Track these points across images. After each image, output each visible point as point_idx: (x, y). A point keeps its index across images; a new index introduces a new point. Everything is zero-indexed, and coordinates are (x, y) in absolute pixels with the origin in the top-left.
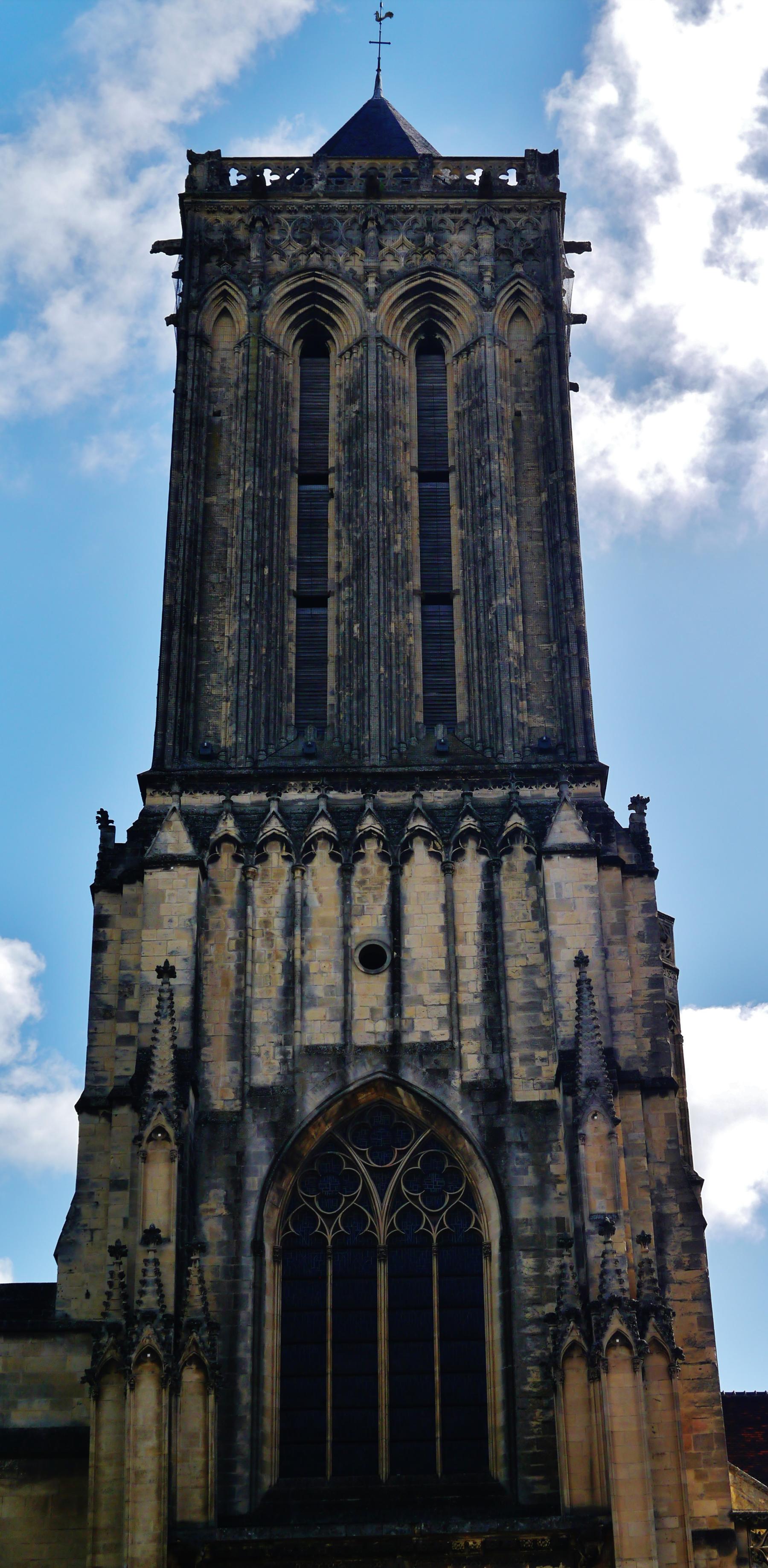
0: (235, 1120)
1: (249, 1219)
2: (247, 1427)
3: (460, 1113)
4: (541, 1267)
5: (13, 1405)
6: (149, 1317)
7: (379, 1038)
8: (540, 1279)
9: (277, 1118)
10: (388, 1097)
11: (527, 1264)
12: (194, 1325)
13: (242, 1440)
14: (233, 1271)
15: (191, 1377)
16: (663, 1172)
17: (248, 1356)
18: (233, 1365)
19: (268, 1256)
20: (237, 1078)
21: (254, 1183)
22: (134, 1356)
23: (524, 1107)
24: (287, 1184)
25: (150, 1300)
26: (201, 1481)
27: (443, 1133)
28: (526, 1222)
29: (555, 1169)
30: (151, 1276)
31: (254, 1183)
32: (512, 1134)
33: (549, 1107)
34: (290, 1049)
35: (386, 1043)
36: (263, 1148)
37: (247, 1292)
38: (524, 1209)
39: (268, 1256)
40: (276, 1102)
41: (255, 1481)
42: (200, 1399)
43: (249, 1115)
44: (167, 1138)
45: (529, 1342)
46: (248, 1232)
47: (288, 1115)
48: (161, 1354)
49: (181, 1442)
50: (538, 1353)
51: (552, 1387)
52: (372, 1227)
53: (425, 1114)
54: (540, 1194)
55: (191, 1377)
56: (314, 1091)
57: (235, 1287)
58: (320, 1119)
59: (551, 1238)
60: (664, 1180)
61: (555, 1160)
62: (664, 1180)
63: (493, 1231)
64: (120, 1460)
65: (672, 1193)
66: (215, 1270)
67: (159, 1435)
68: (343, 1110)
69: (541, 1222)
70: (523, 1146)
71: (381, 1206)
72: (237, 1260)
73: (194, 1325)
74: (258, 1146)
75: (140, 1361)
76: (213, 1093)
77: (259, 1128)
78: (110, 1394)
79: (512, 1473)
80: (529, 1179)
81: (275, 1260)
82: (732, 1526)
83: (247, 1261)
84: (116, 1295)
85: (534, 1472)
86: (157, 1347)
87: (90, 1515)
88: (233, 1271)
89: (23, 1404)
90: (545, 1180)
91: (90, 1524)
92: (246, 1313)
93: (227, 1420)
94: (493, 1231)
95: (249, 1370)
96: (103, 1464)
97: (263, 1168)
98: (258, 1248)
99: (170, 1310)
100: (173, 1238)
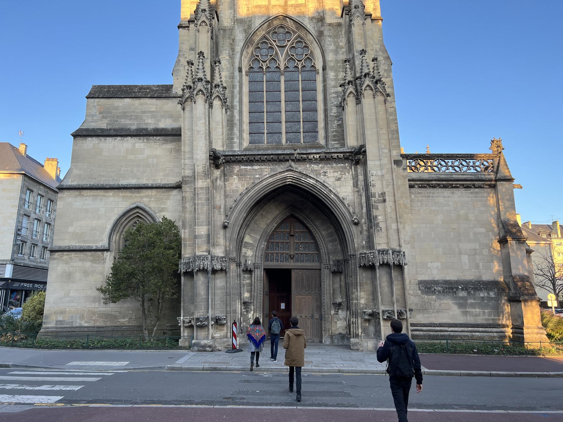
0: (232, 30)
1: (237, 61)
2: (238, 127)
3: (308, 26)
4: (337, 76)
5: (160, 120)
6: (200, 80)
7: (280, 2)
8: (336, 79)
9: (246, 28)
10: (284, 23)
11: (331, 75)
12: (217, 86)
13: (236, 131)
14: (232, 77)
15: (217, 103)
16: (378, 47)
17: (238, 104)
18: (233, 107)
19: (244, 73)
20: (232, 15)
21: (238, 49)
22: (195, 93)
23: (330, 25)
24: (251, 49)
25: (200, 75)
26: (221, 137)
27: (302, 34)
28: (331, 61)
29: (341, 44)
30: (201, 67)
31: (238, 49)
32: (326, 33)
33: (339, 25)
34: (250, 6)
35: (283, 4)
36: (241, 37)
37: (237, 84)
38: (330, 57)
39: (244, 73)
40: (245, 23)
41: (241, 144)
42: (220, 110)
43: (236, 27)
44: (207, 25)
45: (333, 100)
46: (237, 65)
47: (250, 27)
48: (205, 92)
49: (213, 125)
50: (336, 103)
51: (341, 107)
52: (279, 65)
53: (296, 28)
54: (336, 52)
55: (217, 103)
56: (258, 19)
57: (232, 82)
58: (260, 29)
59: (340, 66)
60: (378, 49)
61: (341, 41)
62: (378, 49)
63: (319, 65)
64: (191, 129)
65: (381, 53)
66: (226, 77)
67: (205, 119)
68: (269, 26)
69: (337, 61)
70: (330, 36)
71: (282, 58)
72: (233, 73)
73: (217, 86)
74: (240, 37)
75: (197, 94)
76: (224, 21)
77: (240, 31)
78: (188, 108)
79: (327, 141)
80: (332, 47)
81: (246, 75)
82: (401, 158)
83: (237, 73)
84: (190, 76)
85: (335, 140)
86: (203, 90)
87: (182, 147)
88: (232, 77)
89: (163, 120)
90: (338, 47)
91: (183, 150)
92: (237, 90)
93: (230, 124)
94: (319, 65)
95: (238, 108)
96: (186, 131)
97: (242, 44)
98: (240, 70)
99: (209, 78)
100: (209, 57)
